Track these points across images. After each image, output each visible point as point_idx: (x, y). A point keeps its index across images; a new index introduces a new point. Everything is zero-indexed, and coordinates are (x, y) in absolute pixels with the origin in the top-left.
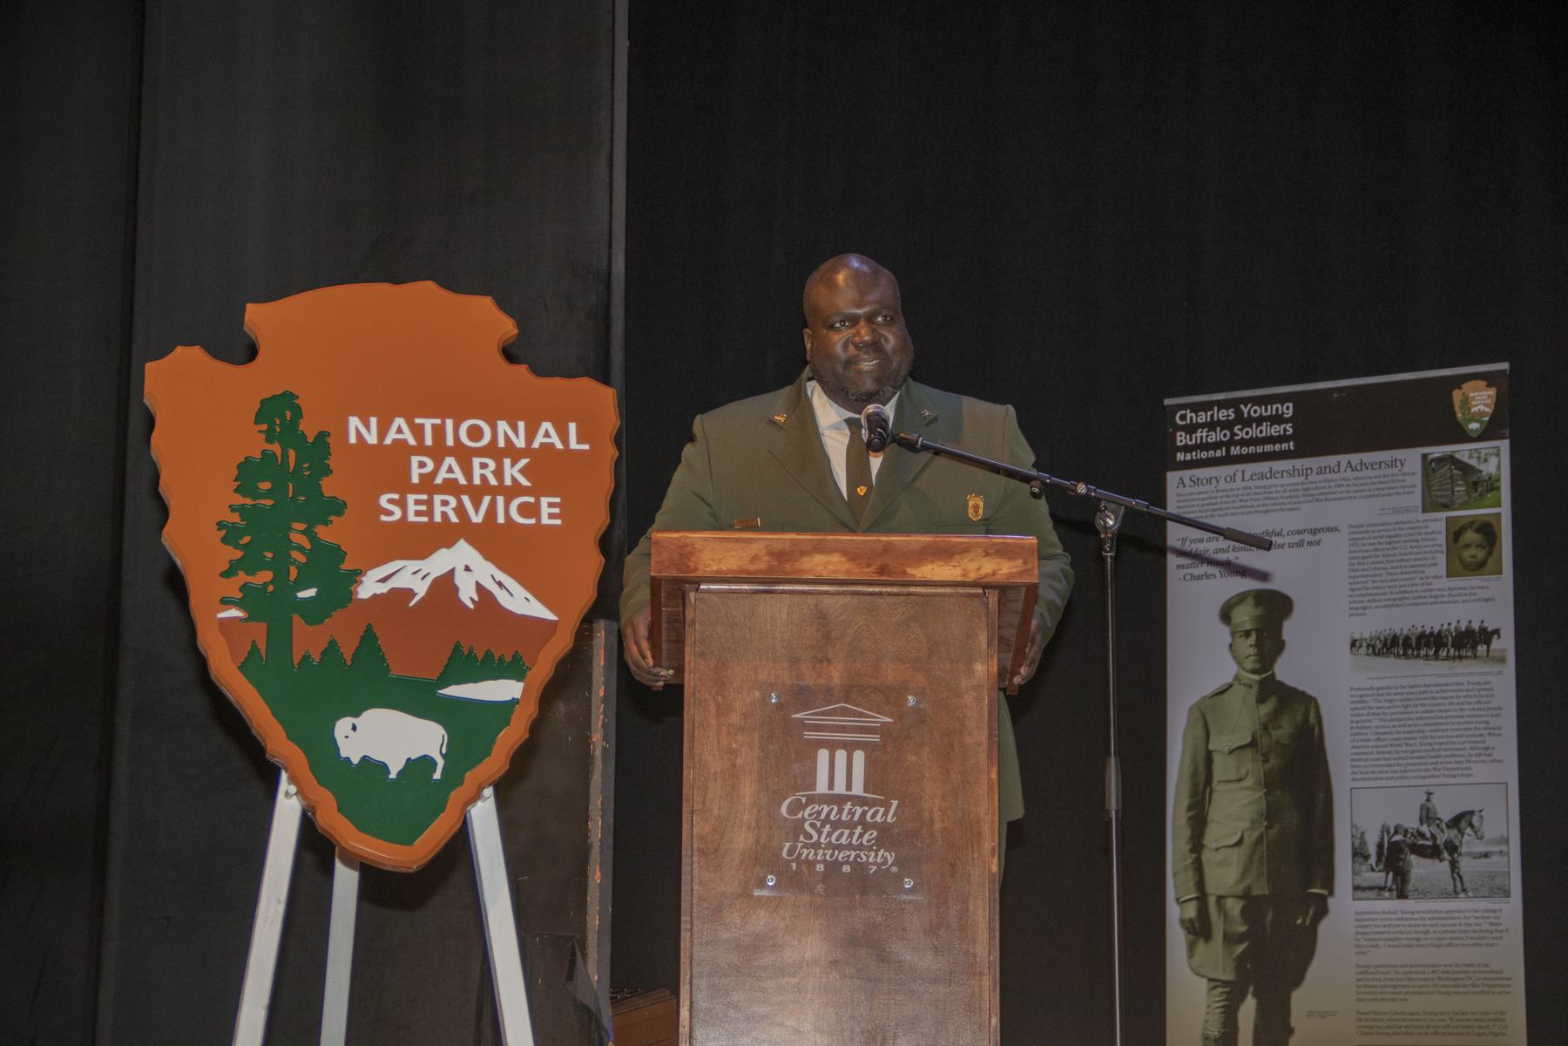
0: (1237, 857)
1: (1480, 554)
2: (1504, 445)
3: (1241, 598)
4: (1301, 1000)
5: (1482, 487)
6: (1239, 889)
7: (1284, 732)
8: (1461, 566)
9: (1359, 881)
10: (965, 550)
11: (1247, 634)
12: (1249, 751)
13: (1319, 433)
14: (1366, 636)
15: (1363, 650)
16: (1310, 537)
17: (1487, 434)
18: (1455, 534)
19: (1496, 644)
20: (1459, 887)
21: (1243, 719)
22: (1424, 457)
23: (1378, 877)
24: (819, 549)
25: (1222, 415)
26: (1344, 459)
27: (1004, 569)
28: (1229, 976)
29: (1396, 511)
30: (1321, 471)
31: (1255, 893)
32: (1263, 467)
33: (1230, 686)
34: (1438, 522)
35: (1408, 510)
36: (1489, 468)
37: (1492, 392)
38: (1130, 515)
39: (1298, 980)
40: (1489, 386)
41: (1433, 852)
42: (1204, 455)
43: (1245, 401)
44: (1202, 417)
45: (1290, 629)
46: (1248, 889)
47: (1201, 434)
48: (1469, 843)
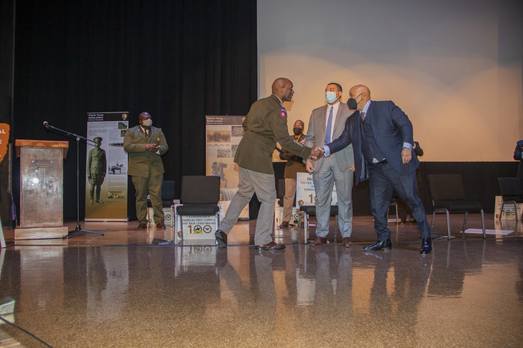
0: (95, 169)
2: (128, 122)
4: (102, 186)
5: (125, 126)
7: (101, 154)
10: (59, 143)
13: (106, 118)
16: (105, 131)
17: (126, 120)
18: (122, 132)
20: (121, 173)
21: (96, 152)
23: (112, 172)
24: (39, 142)
27: (64, 146)
34: (120, 130)
36: (126, 124)
38: (81, 139)
41: (118, 169)
45: (102, 142)
48: (122, 168)
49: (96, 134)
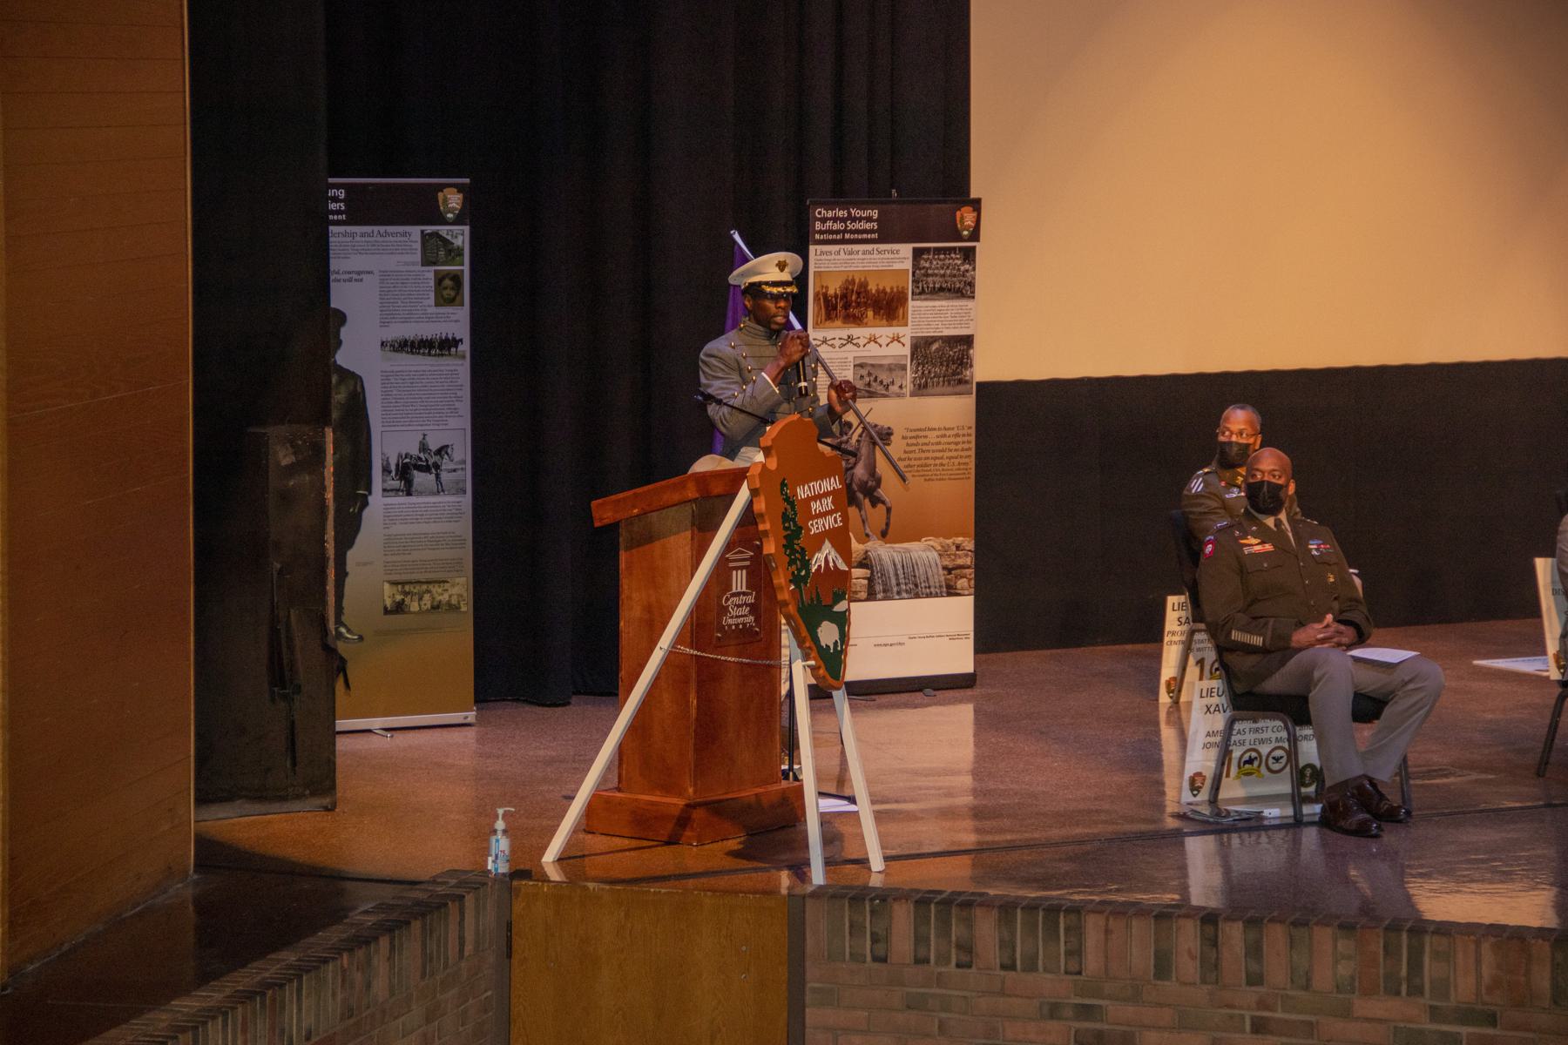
1: (452, 293)
2: (467, 229)
5: (454, 254)
8: (443, 300)
17: (458, 221)
18: (440, 280)
19: (461, 348)
20: (440, 489)
23: (396, 484)
26: (376, 228)
29: (406, 264)
30: (362, 235)
34: (429, 273)
35: (414, 264)
36: (458, 242)
41: (427, 469)
48: (446, 464)
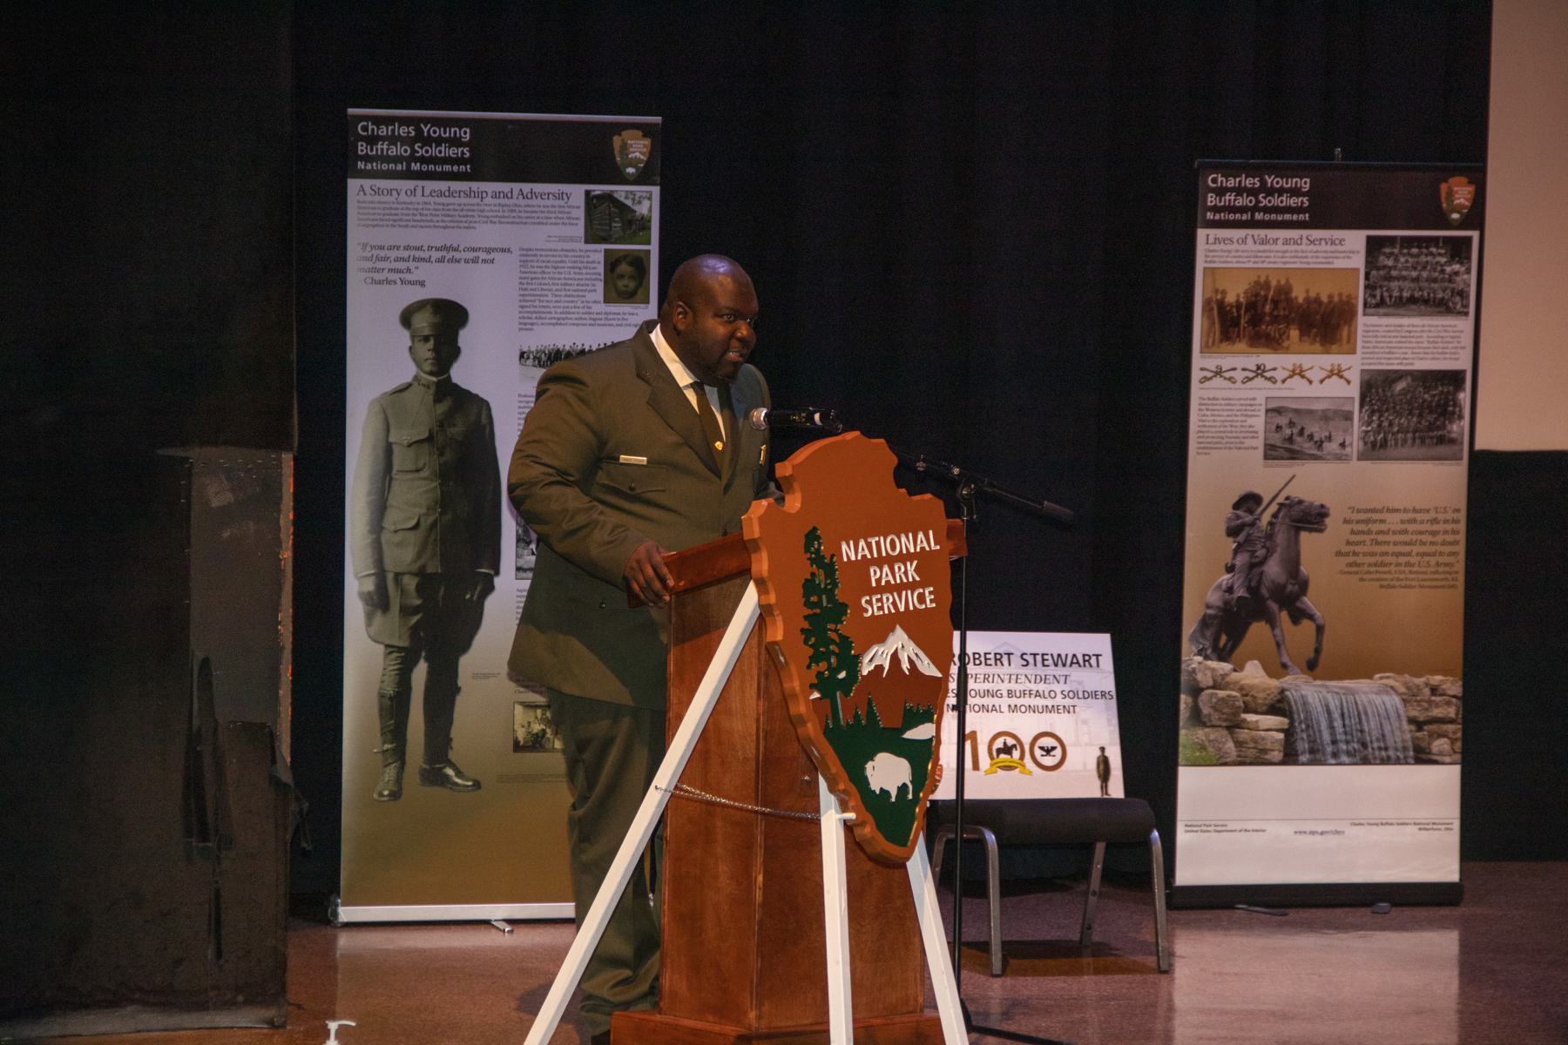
0: (414, 539)
1: (632, 285)
2: (656, 191)
3: (420, 306)
6: (415, 568)
7: (457, 430)
9: (521, 563)
11: (426, 339)
12: (426, 445)
14: (533, 349)
15: (530, 362)
17: (642, 179)
18: (612, 262)
22: (588, 193)
25: (403, 131)
26: (516, 186)
28: (405, 643)
29: (562, 239)
31: (430, 570)
32: (443, 185)
33: (410, 385)
34: (597, 254)
35: (572, 239)
36: (642, 209)
37: (647, 142)
39: (465, 646)
40: (645, 136)
42: (385, 167)
43: (427, 120)
44: (384, 131)
45: (465, 337)
46: (424, 566)
47: (382, 147)
49: (422, 272)
